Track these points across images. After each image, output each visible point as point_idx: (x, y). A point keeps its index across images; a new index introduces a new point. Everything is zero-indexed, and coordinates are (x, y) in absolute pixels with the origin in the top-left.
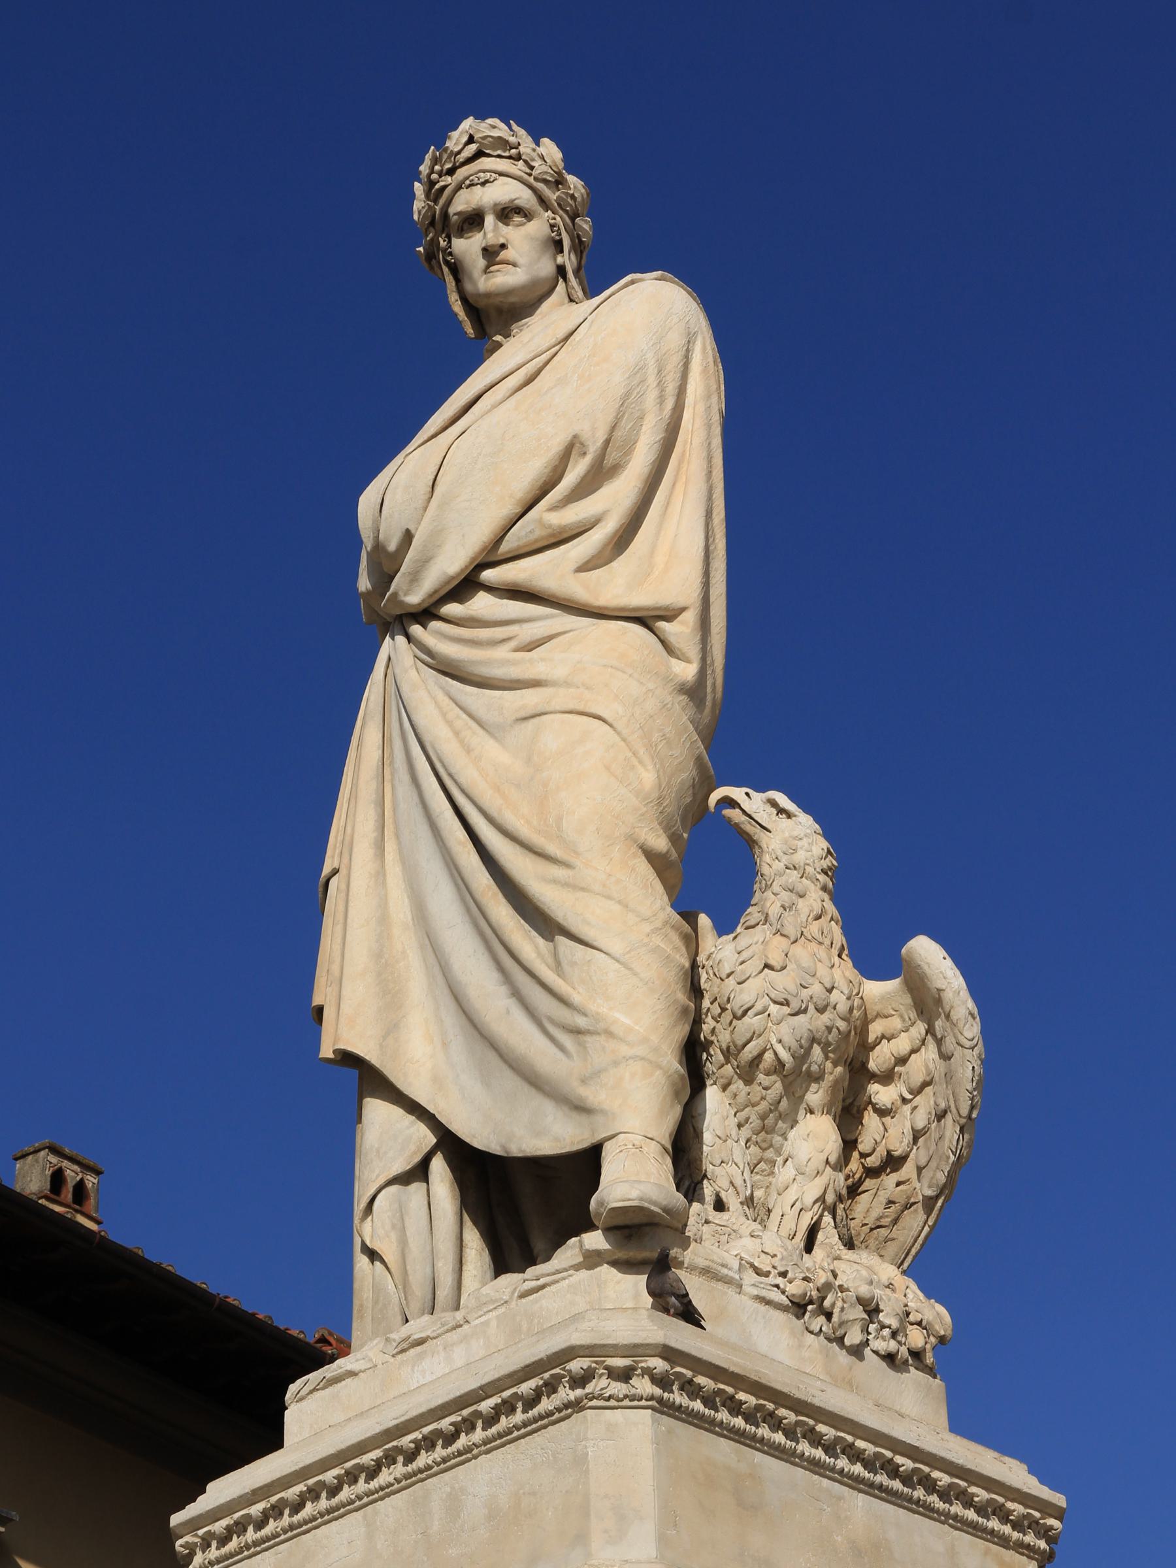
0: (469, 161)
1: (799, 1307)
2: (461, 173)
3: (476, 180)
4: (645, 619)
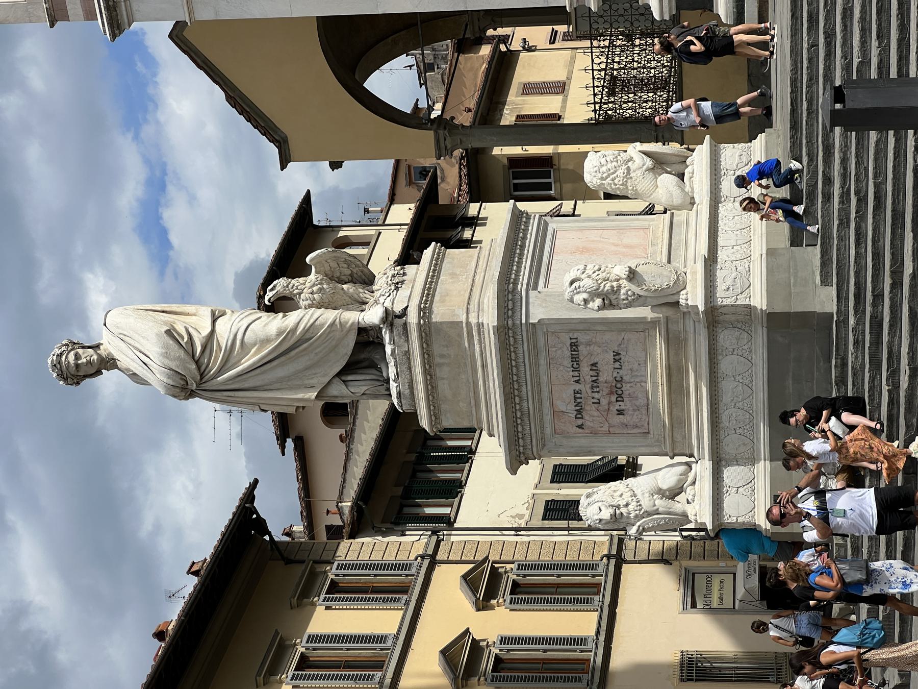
1: (397, 289)
2: (64, 368)
4: (214, 321)
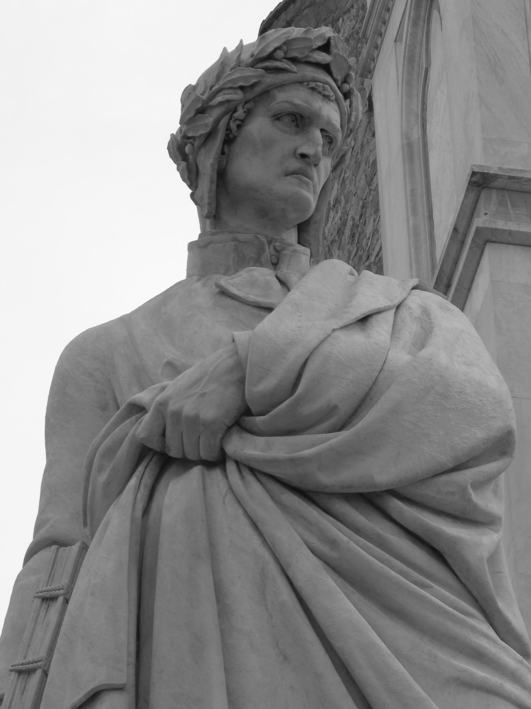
0: (318, 65)
2: (310, 72)
3: (320, 89)
